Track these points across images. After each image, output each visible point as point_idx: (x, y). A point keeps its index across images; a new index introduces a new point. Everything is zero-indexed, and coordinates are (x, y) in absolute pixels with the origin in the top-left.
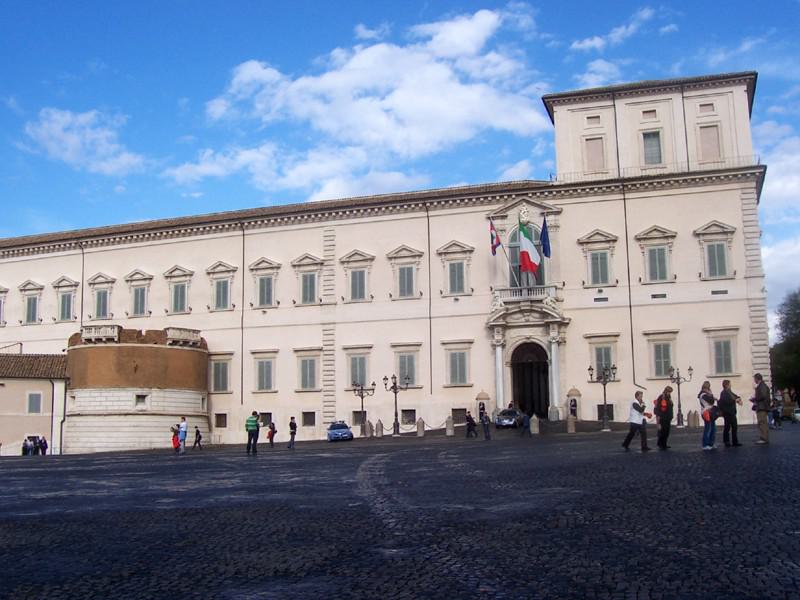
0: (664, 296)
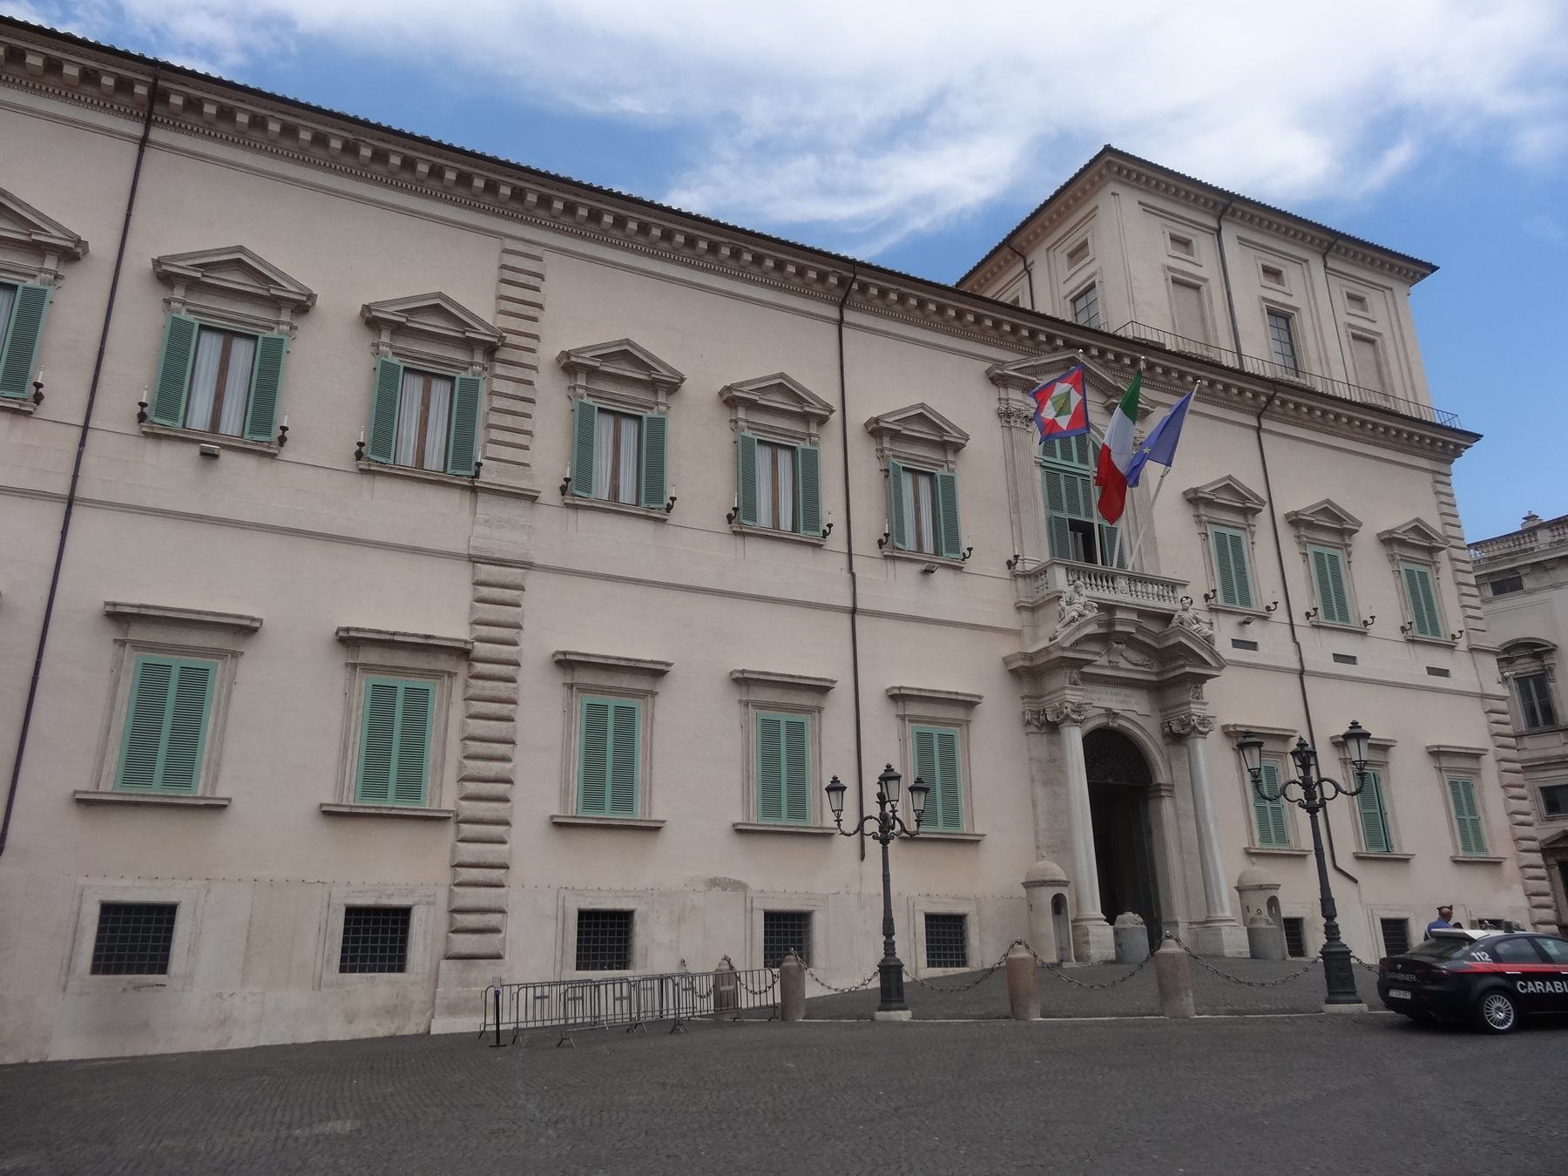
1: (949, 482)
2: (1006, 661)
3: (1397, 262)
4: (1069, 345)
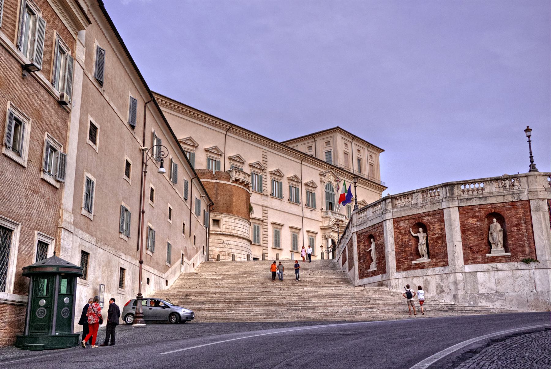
1: (315, 194)
2: (320, 227)
4: (331, 168)
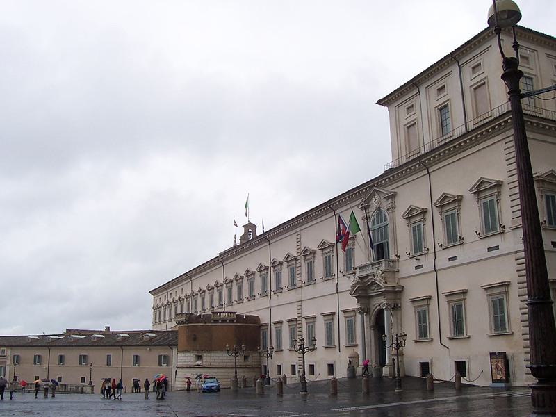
0: (455, 258)
3: (484, 35)
4: (371, 187)
